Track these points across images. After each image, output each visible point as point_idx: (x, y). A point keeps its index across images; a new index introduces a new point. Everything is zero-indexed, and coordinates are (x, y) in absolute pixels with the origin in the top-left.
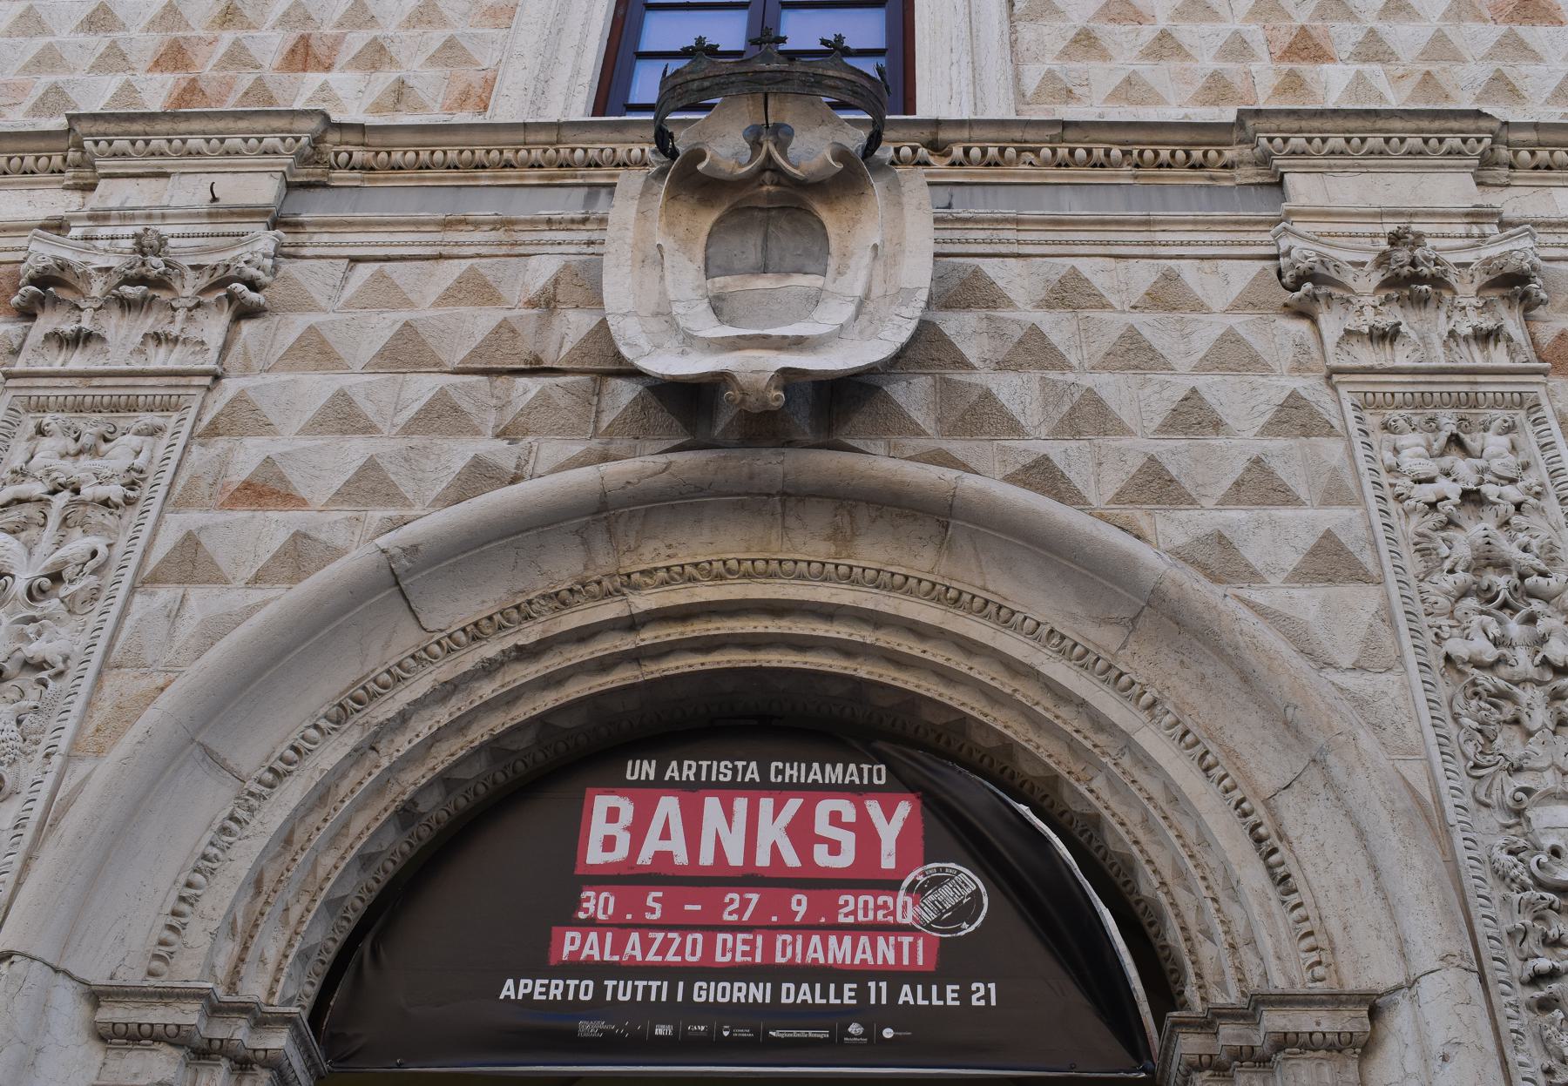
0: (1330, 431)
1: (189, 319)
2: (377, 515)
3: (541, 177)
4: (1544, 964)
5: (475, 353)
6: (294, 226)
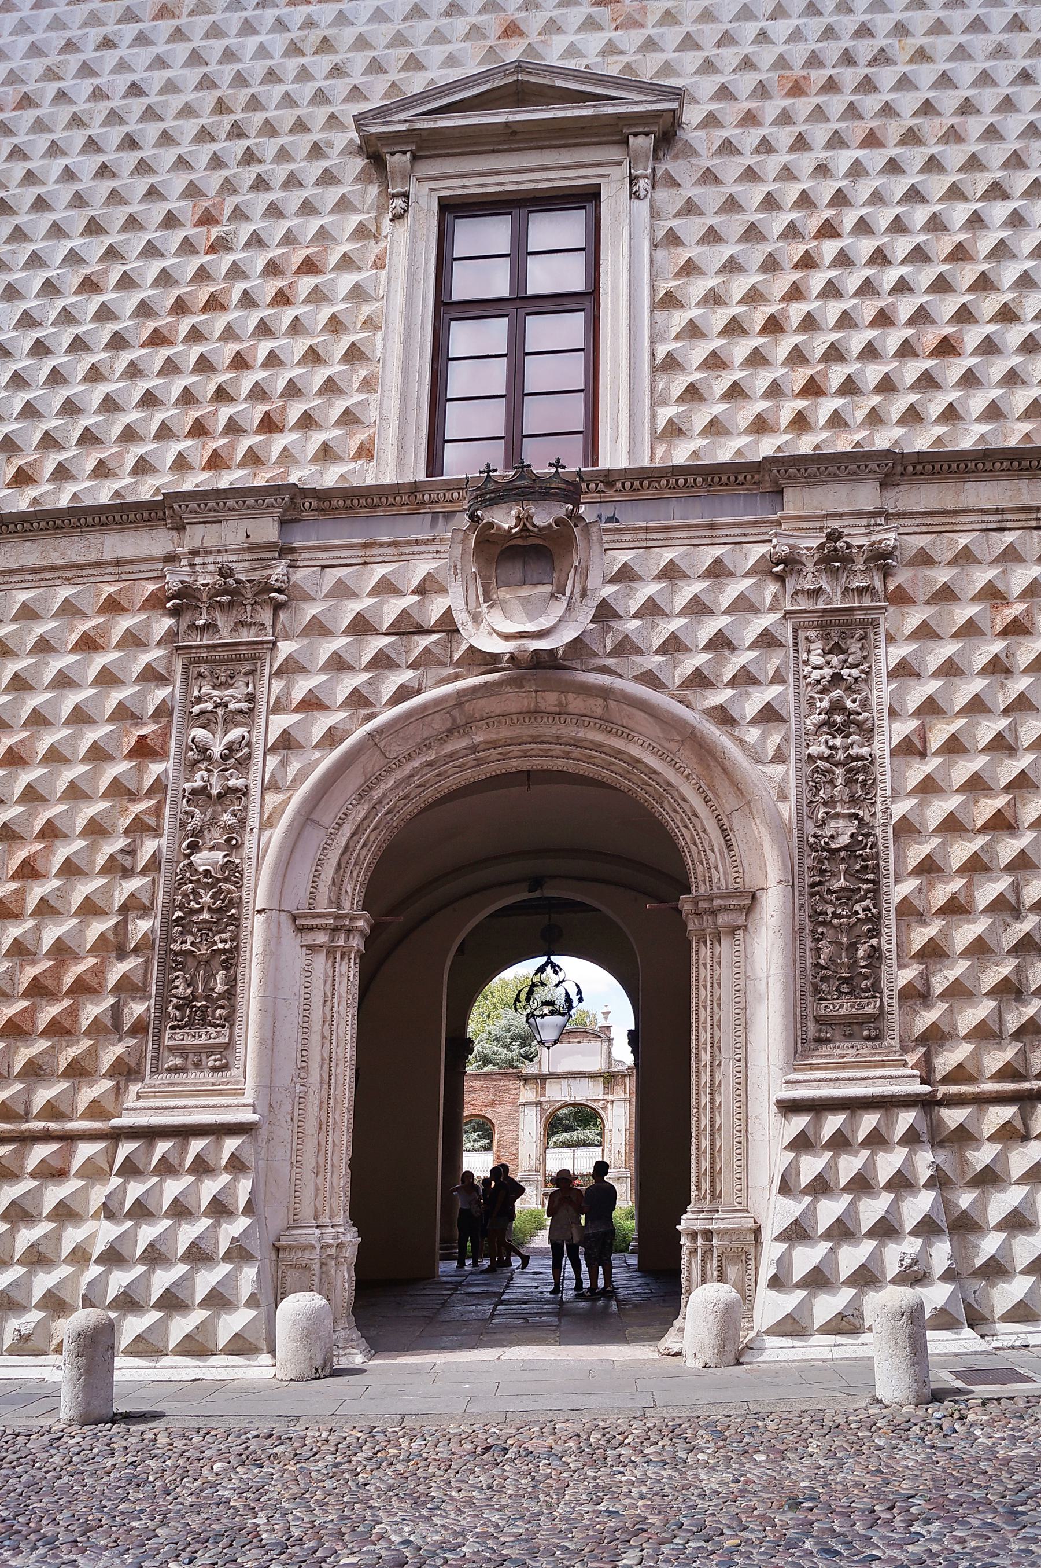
0: (781, 645)
2: (363, 712)
4: (817, 879)
6: (292, 550)
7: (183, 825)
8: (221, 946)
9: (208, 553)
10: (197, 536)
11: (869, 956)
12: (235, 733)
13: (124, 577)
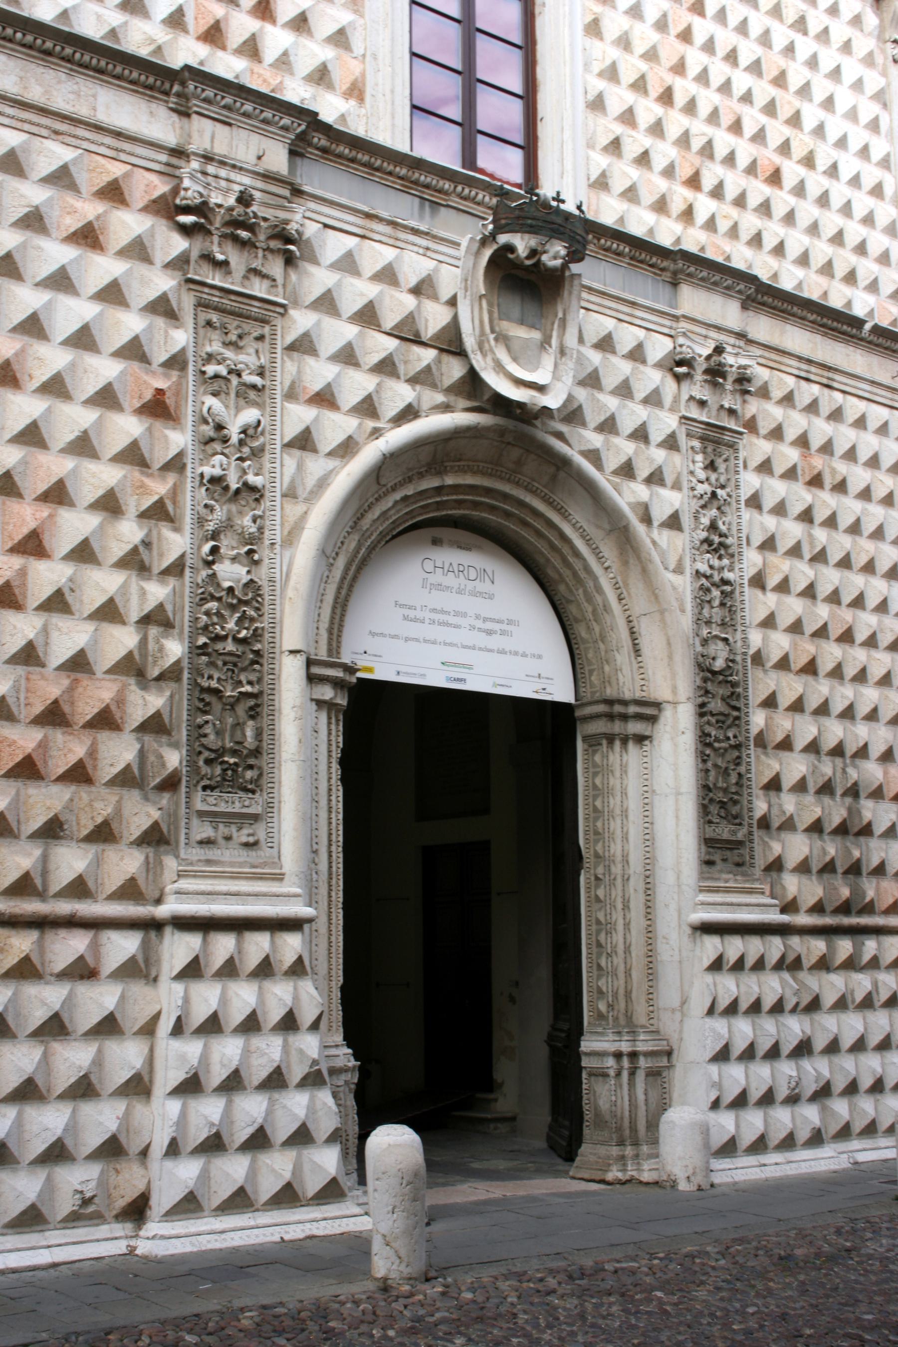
1: (264, 256)
2: (370, 424)
3: (403, 185)
5: (396, 327)
7: (201, 521)
8: (248, 688)
9: (223, 163)
10: (205, 134)
11: (737, 784)
12: (250, 415)
13: (123, 157)
